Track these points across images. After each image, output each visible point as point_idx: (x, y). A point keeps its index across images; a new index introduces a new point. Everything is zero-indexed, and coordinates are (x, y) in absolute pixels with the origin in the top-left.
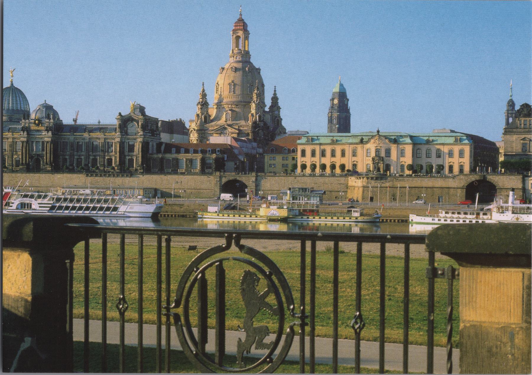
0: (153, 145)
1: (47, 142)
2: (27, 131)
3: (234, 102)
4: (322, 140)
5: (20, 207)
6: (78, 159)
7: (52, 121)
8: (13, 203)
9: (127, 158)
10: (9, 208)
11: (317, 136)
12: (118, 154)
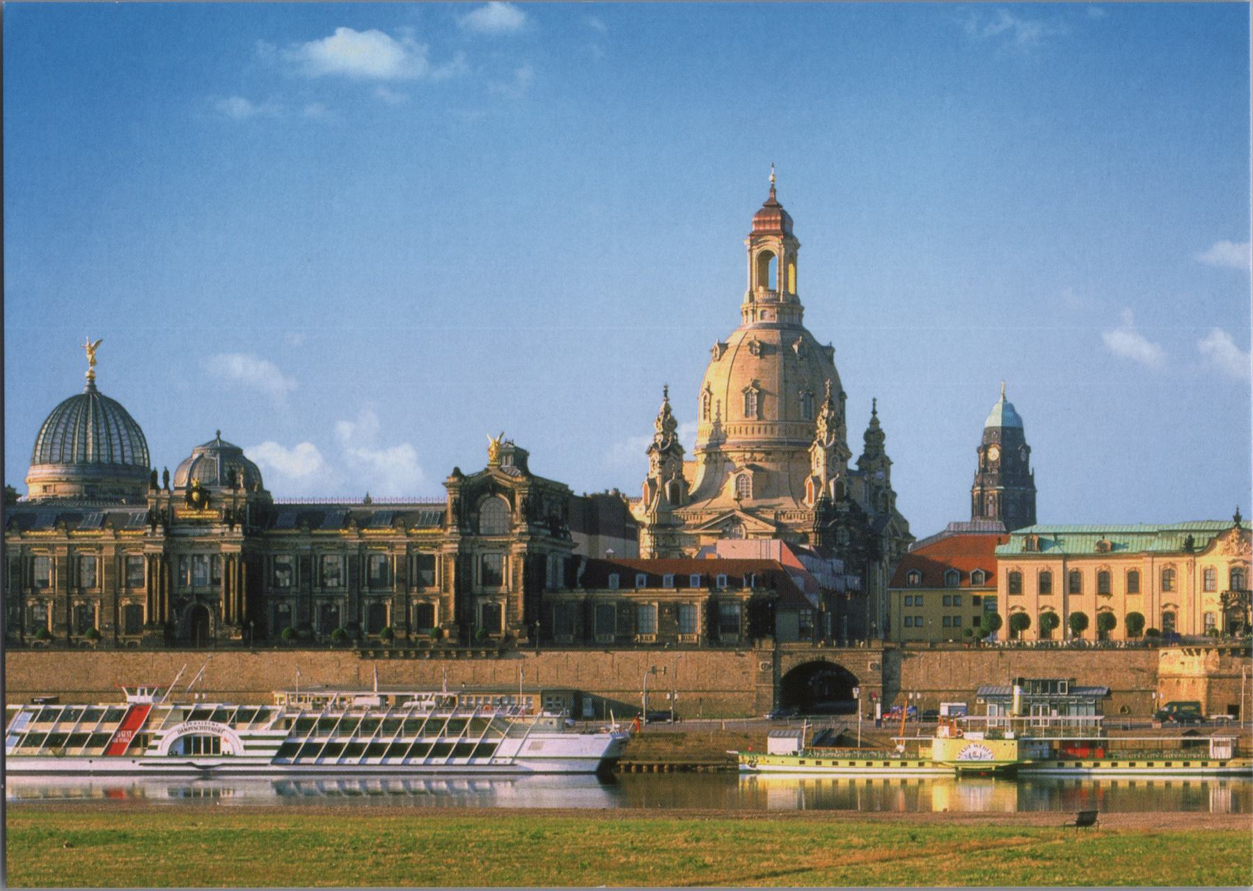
1: (230, 557)
2: (165, 524)
3: (759, 444)
4: (1072, 546)
5: (180, 749)
6: (324, 607)
7: (242, 492)
8: (160, 738)
9: (481, 601)
10: (149, 752)
11: (1055, 534)
12: (452, 590)
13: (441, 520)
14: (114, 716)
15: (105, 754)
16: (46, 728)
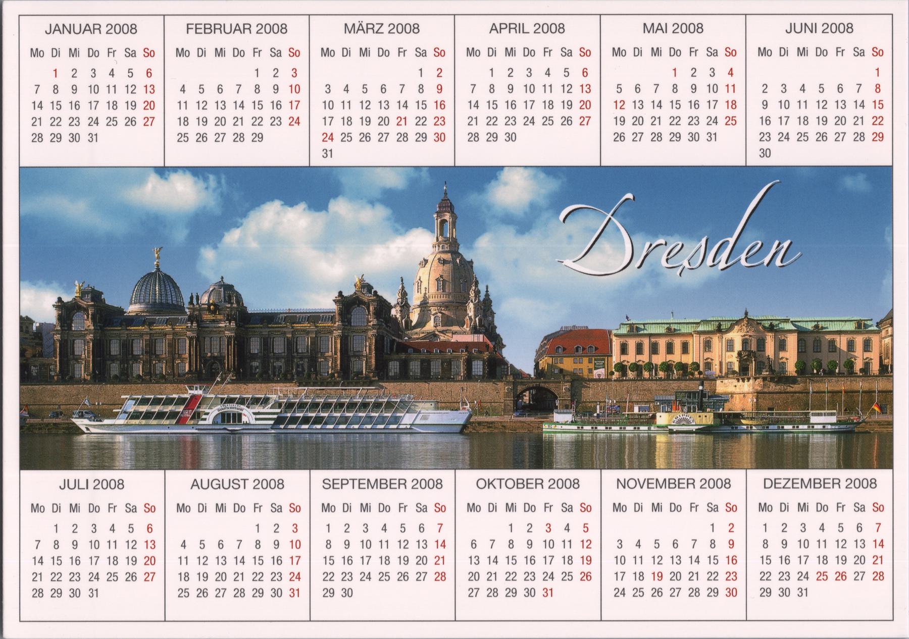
0: (387, 341)
2: (197, 322)
5: (219, 420)
7: (235, 305)
8: (207, 414)
10: (201, 422)
13: (332, 319)
14: (181, 401)
15: (177, 423)
16: (144, 409)
